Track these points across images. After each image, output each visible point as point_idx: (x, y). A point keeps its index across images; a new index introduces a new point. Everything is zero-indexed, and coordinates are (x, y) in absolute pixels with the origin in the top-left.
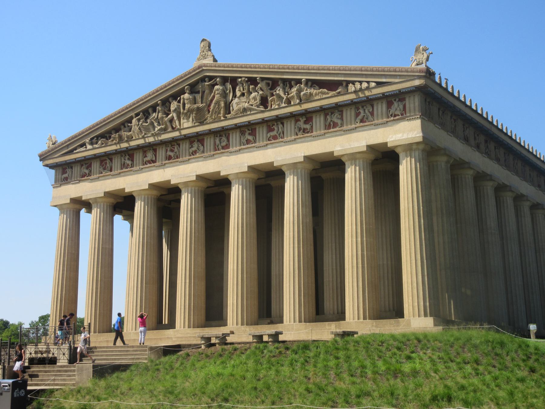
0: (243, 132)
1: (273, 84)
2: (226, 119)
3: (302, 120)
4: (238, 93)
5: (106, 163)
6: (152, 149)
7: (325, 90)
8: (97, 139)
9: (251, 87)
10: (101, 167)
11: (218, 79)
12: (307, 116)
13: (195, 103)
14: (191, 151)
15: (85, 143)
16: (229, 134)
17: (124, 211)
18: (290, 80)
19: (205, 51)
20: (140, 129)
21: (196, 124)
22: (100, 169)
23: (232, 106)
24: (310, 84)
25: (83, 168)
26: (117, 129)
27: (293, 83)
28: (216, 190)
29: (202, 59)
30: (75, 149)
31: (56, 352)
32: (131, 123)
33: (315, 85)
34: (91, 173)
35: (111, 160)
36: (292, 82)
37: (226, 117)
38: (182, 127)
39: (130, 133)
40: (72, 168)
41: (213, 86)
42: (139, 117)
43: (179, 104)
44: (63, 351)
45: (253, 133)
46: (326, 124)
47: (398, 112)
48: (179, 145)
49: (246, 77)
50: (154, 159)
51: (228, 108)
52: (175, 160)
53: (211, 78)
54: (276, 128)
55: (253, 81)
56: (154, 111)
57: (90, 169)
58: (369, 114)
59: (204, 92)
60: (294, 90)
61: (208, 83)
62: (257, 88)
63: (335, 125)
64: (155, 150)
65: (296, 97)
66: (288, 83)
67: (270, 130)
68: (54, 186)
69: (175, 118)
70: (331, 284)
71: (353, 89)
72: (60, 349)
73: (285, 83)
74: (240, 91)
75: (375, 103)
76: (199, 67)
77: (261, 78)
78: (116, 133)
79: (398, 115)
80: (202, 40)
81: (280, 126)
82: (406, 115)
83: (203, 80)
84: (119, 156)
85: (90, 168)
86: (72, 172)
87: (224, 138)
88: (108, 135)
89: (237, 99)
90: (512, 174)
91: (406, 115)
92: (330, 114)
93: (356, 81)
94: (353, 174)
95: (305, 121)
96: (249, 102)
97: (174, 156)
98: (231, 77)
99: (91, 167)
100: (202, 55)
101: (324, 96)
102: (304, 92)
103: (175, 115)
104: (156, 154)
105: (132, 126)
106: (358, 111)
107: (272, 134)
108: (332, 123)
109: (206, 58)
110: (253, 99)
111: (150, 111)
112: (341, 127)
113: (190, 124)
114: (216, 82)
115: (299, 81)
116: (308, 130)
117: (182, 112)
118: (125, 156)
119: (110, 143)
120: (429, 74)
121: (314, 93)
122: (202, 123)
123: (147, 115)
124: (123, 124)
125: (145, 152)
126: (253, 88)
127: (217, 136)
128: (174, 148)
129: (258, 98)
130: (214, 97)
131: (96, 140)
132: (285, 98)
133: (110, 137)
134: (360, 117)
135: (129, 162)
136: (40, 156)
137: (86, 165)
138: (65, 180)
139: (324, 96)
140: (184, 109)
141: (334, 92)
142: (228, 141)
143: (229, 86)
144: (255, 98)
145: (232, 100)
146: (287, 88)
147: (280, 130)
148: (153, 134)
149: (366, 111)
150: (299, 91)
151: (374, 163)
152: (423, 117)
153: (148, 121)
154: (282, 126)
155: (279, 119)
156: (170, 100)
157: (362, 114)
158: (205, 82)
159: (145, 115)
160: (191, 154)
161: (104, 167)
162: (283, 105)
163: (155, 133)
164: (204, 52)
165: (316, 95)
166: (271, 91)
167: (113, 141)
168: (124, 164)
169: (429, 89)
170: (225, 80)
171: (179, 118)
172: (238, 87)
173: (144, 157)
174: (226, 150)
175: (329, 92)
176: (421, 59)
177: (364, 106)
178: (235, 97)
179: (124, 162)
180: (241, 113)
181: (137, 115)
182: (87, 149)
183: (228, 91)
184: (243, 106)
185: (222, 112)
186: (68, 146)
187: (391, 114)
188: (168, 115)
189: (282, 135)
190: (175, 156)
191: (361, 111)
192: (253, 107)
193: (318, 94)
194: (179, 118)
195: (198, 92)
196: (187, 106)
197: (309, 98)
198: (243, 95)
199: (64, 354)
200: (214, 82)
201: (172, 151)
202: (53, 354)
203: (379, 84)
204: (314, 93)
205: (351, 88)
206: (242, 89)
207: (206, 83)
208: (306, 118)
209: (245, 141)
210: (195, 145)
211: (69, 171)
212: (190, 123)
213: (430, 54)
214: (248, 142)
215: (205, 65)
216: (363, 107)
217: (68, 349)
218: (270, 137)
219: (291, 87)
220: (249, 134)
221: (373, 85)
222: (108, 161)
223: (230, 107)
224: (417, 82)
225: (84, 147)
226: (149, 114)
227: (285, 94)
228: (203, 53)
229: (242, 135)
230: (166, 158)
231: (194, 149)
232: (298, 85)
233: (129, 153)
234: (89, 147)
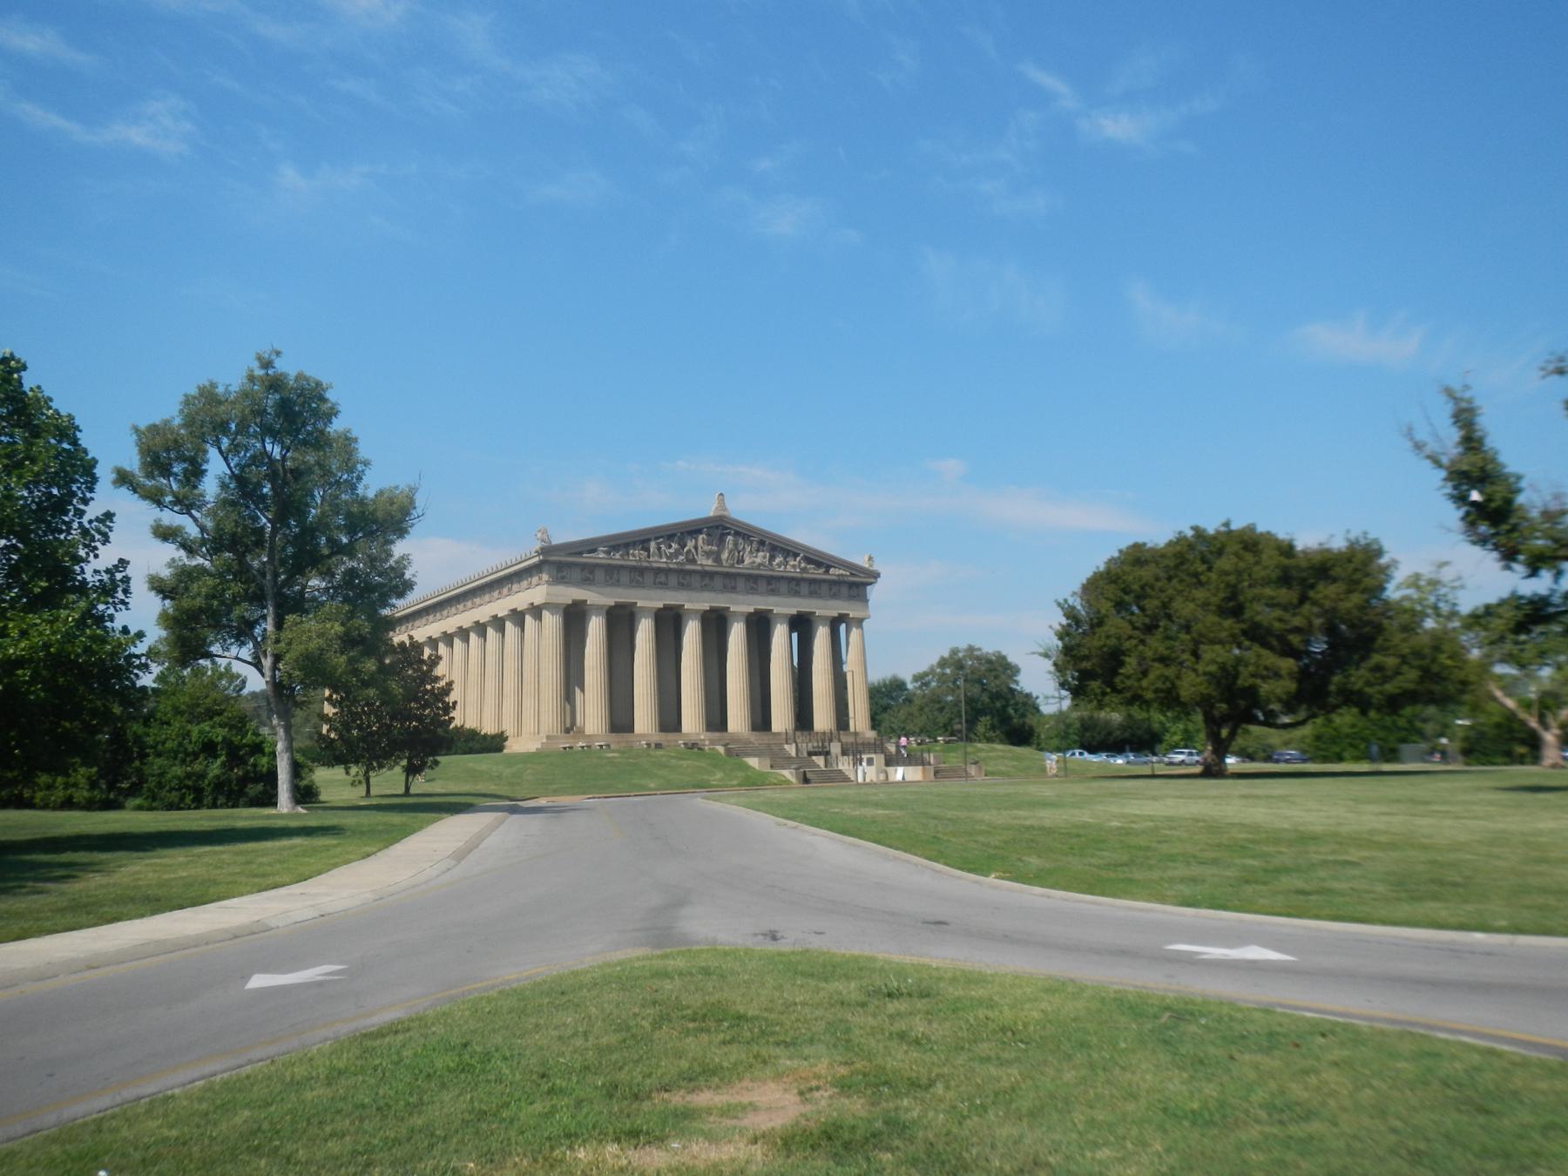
3: (794, 583)
26: (627, 546)
45: (755, 582)
63: (816, 593)
64: (667, 575)
83: (717, 527)
170: (737, 534)
210: (707, 581)
214: (752, 588)
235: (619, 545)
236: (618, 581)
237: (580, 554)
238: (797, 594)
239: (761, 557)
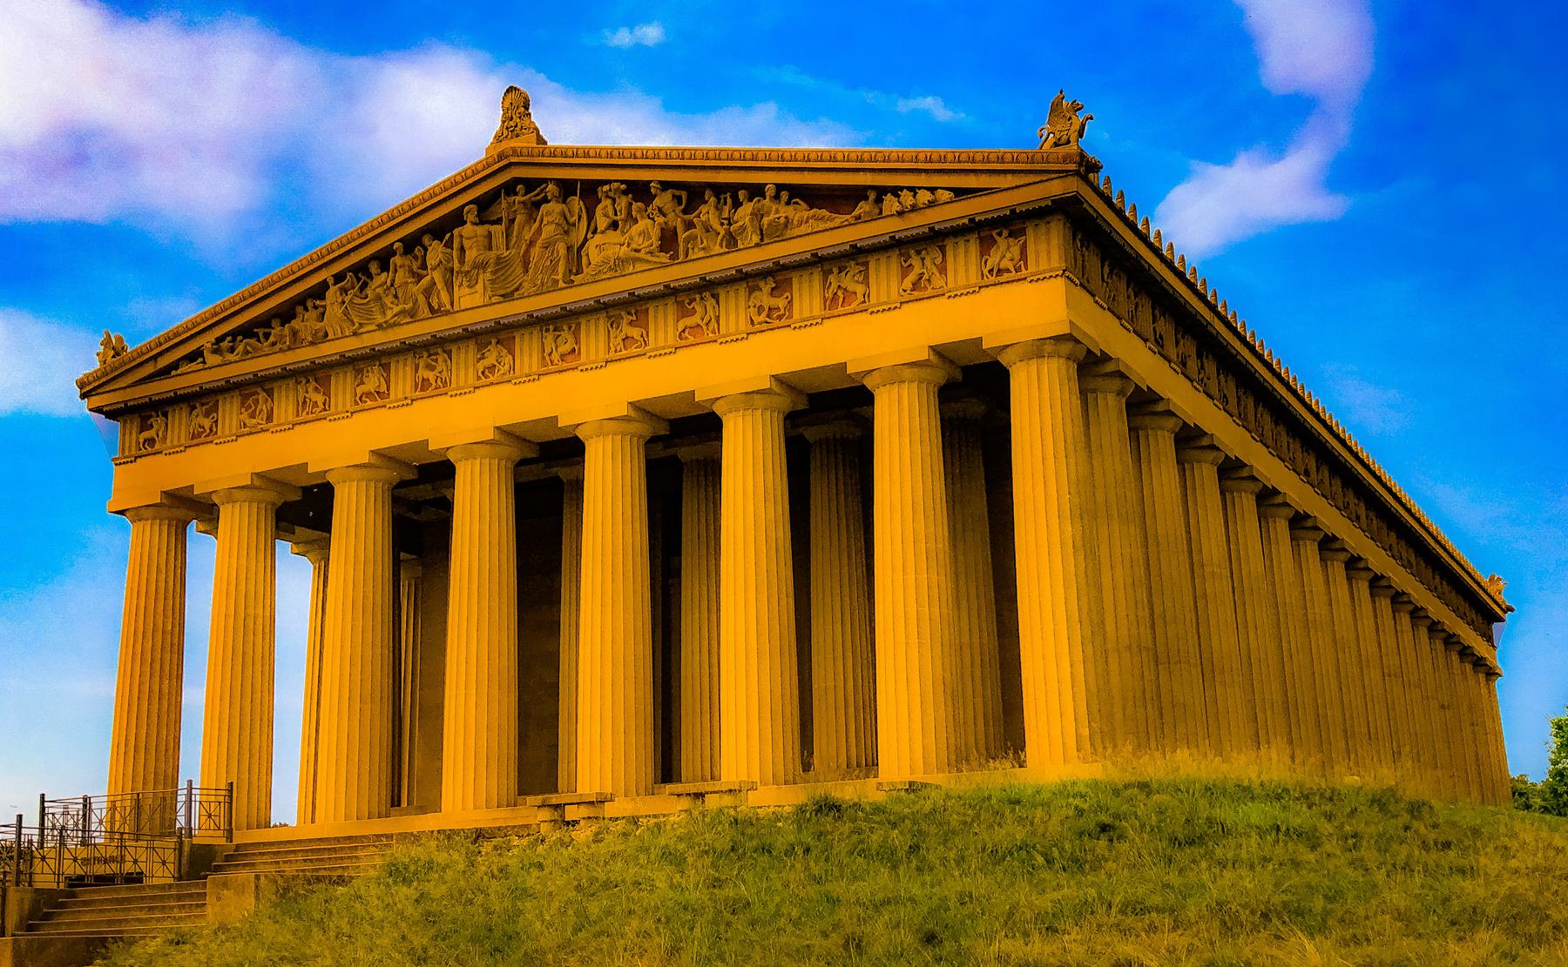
0: (613, 319)
1: (692, 196)
2: (570, 284)
4: (602, 222)
5: (256, 402)
6: (378, 364)
7: (824, 212)
8: (234, 340)
9: (636, 206)
10: (243, 410)
11: (551, 187)
12: (779, 275)
13: (490, 248)
14: (481, 366)
15: (202, 352)
16: (579, 324)
17: (298, 530)
18: (734, 188)
19: (514, 117)
20: (346, 313)
21: (494, 300)
22: (241, 417)
23: (587, 255)
24: (785, 195)
25: (195, 413)
26: (286, 314)
27: (742, 194)
28: (535, 472)
29: (506, 137)
30: (175, 365)
31: (143, 858)
32: (323, 298)
33: (797, 200)
34: (217, 427)
35: (270, 393)
36: (740, 193)
37: (573, 281)
38: (456, 309)
39: (322, 324)
40: (165, 415)
41: (537, 205)
42: (343, 283)
43: (449, 250)
44: (160, 854)
46: (827, 295)
47: (1006, 264)
48: (449, 353)
49: (622, 182)
50: (383, 388)
51: (576, 256)
52: (437, 392)
53: (531, 184)
54: (698, 309)
55: (639, 191)
56: (385, 267)
57: (213, 418)
58: (934, 270)
59: (512, 221)
60: (747, 208)
61: (522, 199)
62: (649, 210)
65: (749, 229)
66: (729, 193)
67: (684, 313)
68: (118, 462)
69: (440, 285)
70: (831, 696)
71: (896, 207)
72: (153, 848)
73: (722, 196)
74: (606, 215)
75: (949, 244)
76: (501, 156)
77: (661, 182)
78: (283, 325)
79: (1008, 271)
80: (508, 91)
81: (711, 302)
82: (1027, 269)
83: (509, 188)
84: (291, 382)
85: (215, 415)
86: (167, 425)
87: (566, 334)
88: (261, 332)
89: (598, 236)
90: (1253, 437)
91: (1027, 269)
92: (835, 270)
93: (902, 189)
94: (896, 418)
95: (773, 289)
96: (629, 245)
97: (436, 382)
98: (583, 182)
99: (217, 411)
100: (507, 128)
101: (822, 226)
102: (772, 217)
103: (437, 276)
104: (389, 376)
105: (324, 307)
106: (908, 263)
107: (689, 321)
108: (840, 293)
109: (517, 136)
110: (640, 235)
111: (374, 268)
112: (864, 302)
113: (478, 299)
114: (543, 195)
115: (756, 191)
116: (782, 312)
117: (456, 269)
118: (308, 381)
119: (267, 350)
120: (1087, 168)
121: (796, 218)
122: (507, 297)
123: (363, 278)
124: (301, 300)
125: (359, 372)
126: (639, 211)
127: (547, 330)
128: (436, 361)
129: (655, 234)
130: (539, 231)
131: (229, 342)
132: (722, 233)
133: (267, 336)
134: (912, 277)
135: (320, 398)
136: (81, 384)
137: (204, 408)
138: (146, 446)
139: (822, 226)
140: (462, 261)
141: (848, 217)
142: (577, 342)
143: (576, 203)
144: (644, 234)
145: (586, 240)
146: (727, 208)
147: (710, 312)
148: (380, 326)
149: (928, 262)
150: (758, 215)
151: (947, 395)
152: (1071, 276)
153: (369, 291)
154: (713, 301)
155: (708, 287)
156: (426, 240)
157: (917, 270)
158: (516, 194)
159: (359, 280)
160: (480, 374)
161: (250, 411)
162: (717, 249)
163: (386, 322)
164: (512, 119)
165: (800, 223)
166: (687, 217)
167: (274, 344)
168: (304, 402)
169: (1085, 205)
170: (567, 188)
171: (449, 286)
172: (600, 207)
173: (358, 385)
174: (573, 365)
175: (834, 215)
176: (1066, 133)
177: (922, 250)
178: (595, 232)
179: (305, 397)
180: (610, 269)
181: (339, 278)
182: (207, 366)
183: (576, 217)
184: (614, 254)
185: (561, 268)
186: (155, 358)
187: (989, 267)
188: (420, 278)
189: (714, 324)
190: (439, 380)
191: (916, 261)
192: (642, 255)
193: (807, 222)
194: (449, 286)
195: (498, 221)
196: (471, 255)
197: (779, 232)
198: (614, 225)
199: (164, 863)
200: (537, 195)
201: (431, 368)
202: (135, 862)
203: (959, 193)
204: (796, 218)
205: (890, 203)
206: (611, 213)
207: (518, 198)
208: (775, 282)
209: (619, 340)
211: (158, 422)
212: (477, 295)
213: (1087, 119)
215: (515, 152)
216: (918, 253)
217: (175, 849)
218: (684, 331)
219: (737, 204)
220: (631, 323)
221: (946, 196)
222: (262, 396)
223: (579, 257)
224: (1057, 188)
225: (200, 360)
226: (370, 277)
227: (722, 224)
228: (511, 123)
229: (612, 326)
230: (416, 385)
231: (486, 362)
232: (756, 199)
233: (317, 373)
234: (212, 359)
235: (264, 322)
236: (269, 419)
237: (165, 373)
238: (774, 318)
239: (644, 231)
